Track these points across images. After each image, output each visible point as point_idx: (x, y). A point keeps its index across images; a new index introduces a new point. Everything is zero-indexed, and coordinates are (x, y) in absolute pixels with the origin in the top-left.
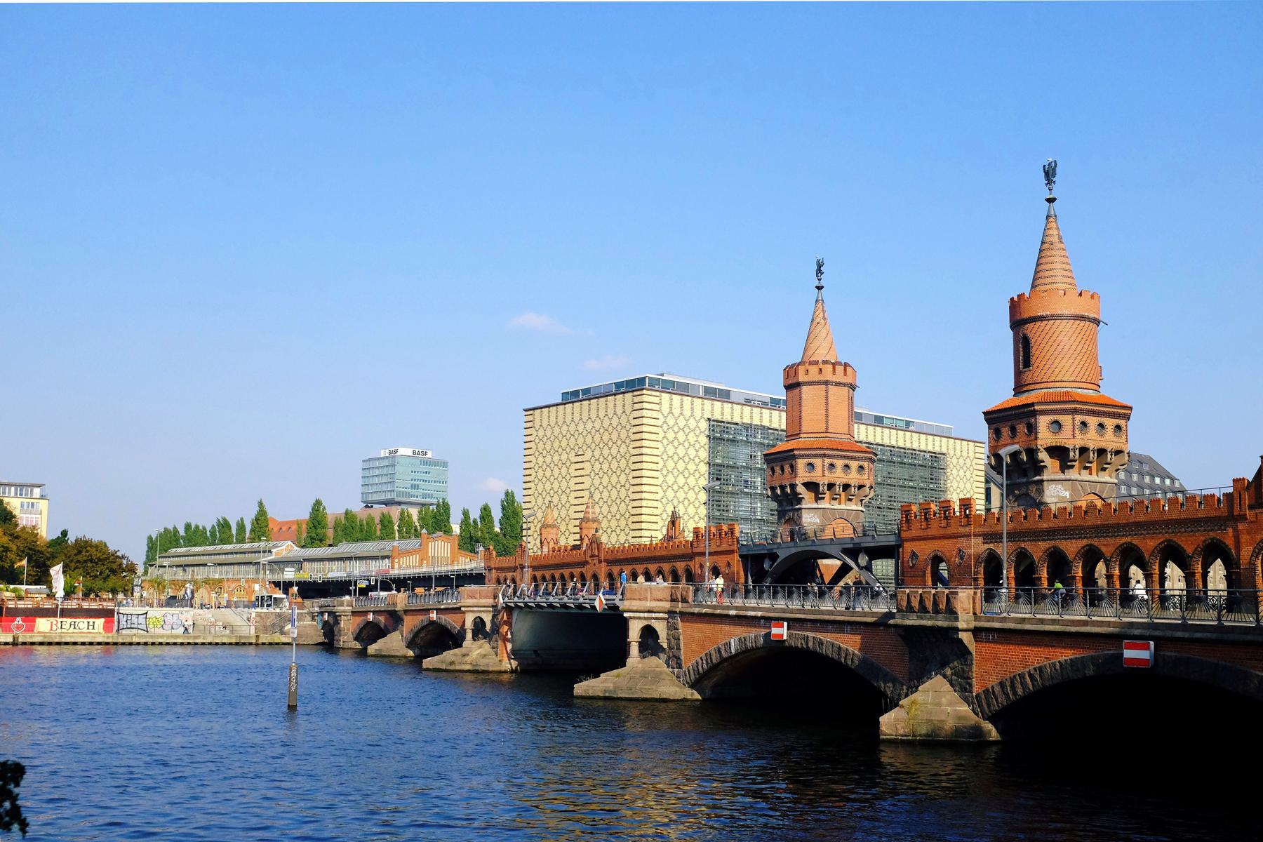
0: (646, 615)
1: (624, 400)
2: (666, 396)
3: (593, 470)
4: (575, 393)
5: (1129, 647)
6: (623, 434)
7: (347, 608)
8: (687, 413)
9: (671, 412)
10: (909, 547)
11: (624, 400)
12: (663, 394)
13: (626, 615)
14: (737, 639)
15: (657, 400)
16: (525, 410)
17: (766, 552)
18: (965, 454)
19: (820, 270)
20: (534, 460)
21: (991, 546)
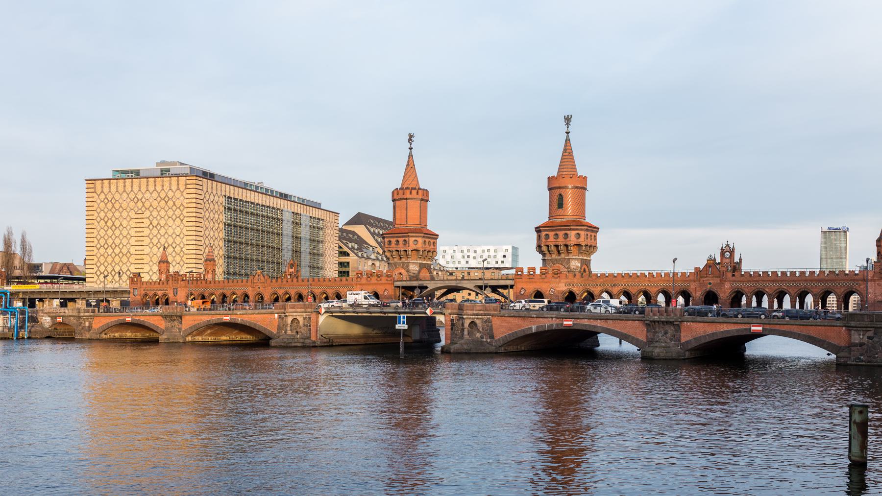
0: (473, 317)
1: (178, 182)
2: (205, 180)
3: (151, 223)
4: (125, 172)
5: (753, 326)
6: (178, 203)
7: (91, 314)
8: (214, 192)
9: (207, 191)
10: (518, 286)
11: (178, 182)
12: (204, 179)
13: (464, 317)
14: (535, 326)
15: (201, 183)
16: (86, 180)
17: (418, 285)
18: (331, 220)
19: (411, 140)
20: (96, 215)
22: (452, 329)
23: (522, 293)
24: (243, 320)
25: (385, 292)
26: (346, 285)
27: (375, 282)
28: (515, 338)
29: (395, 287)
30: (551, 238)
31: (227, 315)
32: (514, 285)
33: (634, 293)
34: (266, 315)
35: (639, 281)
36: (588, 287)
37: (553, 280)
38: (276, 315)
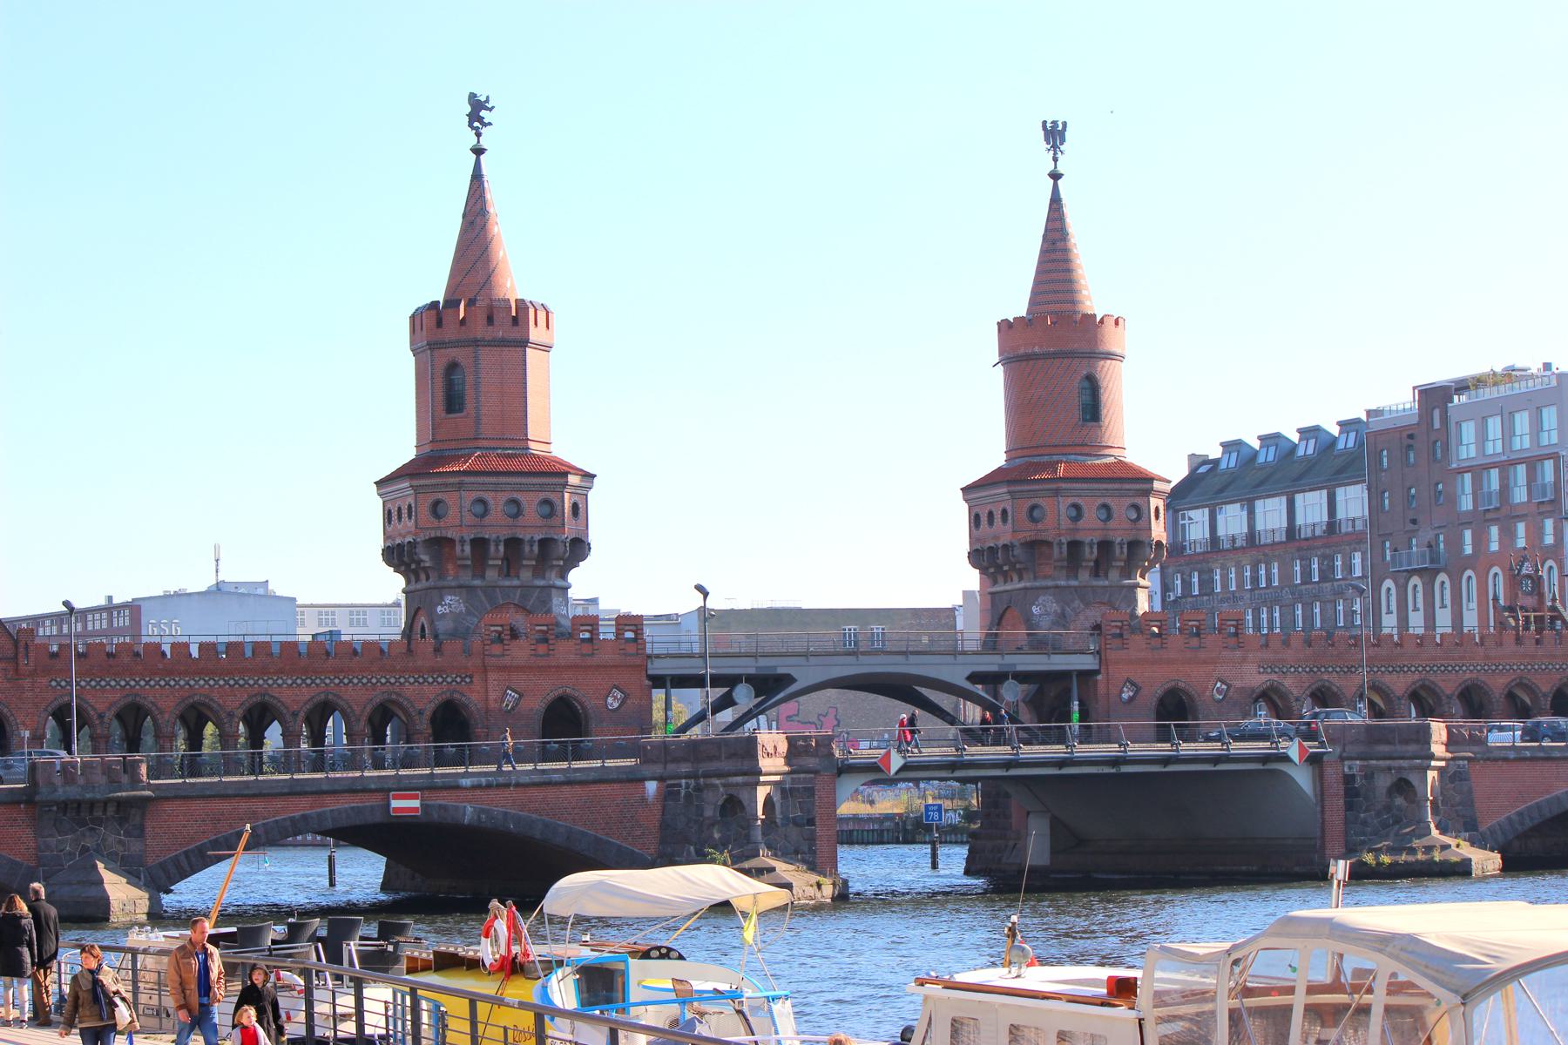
17: (752, 671)
19: (481, 120)
22: (1349, 806)
23: (1125, 696)
24: (483, 811)
25: (610, 700)
26: (432, 671)
27: (573, 658)
28: (1536, 822)
30: (1091, 517)
31: (405, 788)
32: (1097, 672)
33: (1448, 692)
34: (602, 787)
35: (1461, 658)
36: (1326, 677)
37: (1225, 653)
38: (651, 786)
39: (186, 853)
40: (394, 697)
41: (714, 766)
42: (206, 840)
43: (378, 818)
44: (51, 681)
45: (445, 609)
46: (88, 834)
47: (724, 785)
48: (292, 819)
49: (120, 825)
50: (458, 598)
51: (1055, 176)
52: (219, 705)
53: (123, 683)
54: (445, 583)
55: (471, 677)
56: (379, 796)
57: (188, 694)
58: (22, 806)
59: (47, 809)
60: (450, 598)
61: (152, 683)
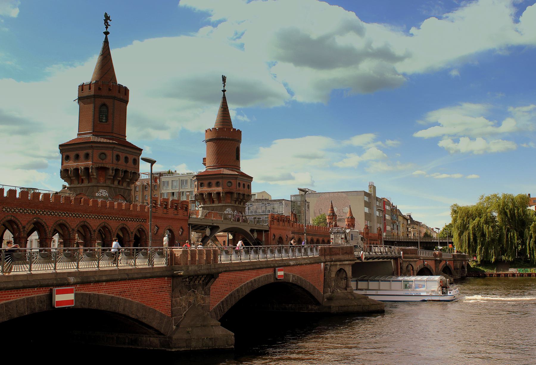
21: (293, 235)
29: (189, 224)
39: (222, 302)
40: (125, 226)
41: (337, 257)
42: (228, 295)
43: (272, 280)
44: (3, 208)
45: (99, 194)
46: (192, 294)
47: (340, 265)
48: (251, 282)
49: (203, 289)
50: (105, 191)
51: (224, 91)
52: (69, 225)
53: (33, 212)
54: (99, 184)
55: (146, 220)
56: (272, 269)
57: (58, 219)
58: (166, 278)
59: (185, 280)
60: (102, 190)
61: (45, 213)
